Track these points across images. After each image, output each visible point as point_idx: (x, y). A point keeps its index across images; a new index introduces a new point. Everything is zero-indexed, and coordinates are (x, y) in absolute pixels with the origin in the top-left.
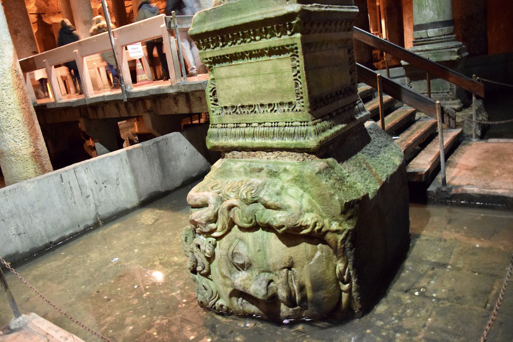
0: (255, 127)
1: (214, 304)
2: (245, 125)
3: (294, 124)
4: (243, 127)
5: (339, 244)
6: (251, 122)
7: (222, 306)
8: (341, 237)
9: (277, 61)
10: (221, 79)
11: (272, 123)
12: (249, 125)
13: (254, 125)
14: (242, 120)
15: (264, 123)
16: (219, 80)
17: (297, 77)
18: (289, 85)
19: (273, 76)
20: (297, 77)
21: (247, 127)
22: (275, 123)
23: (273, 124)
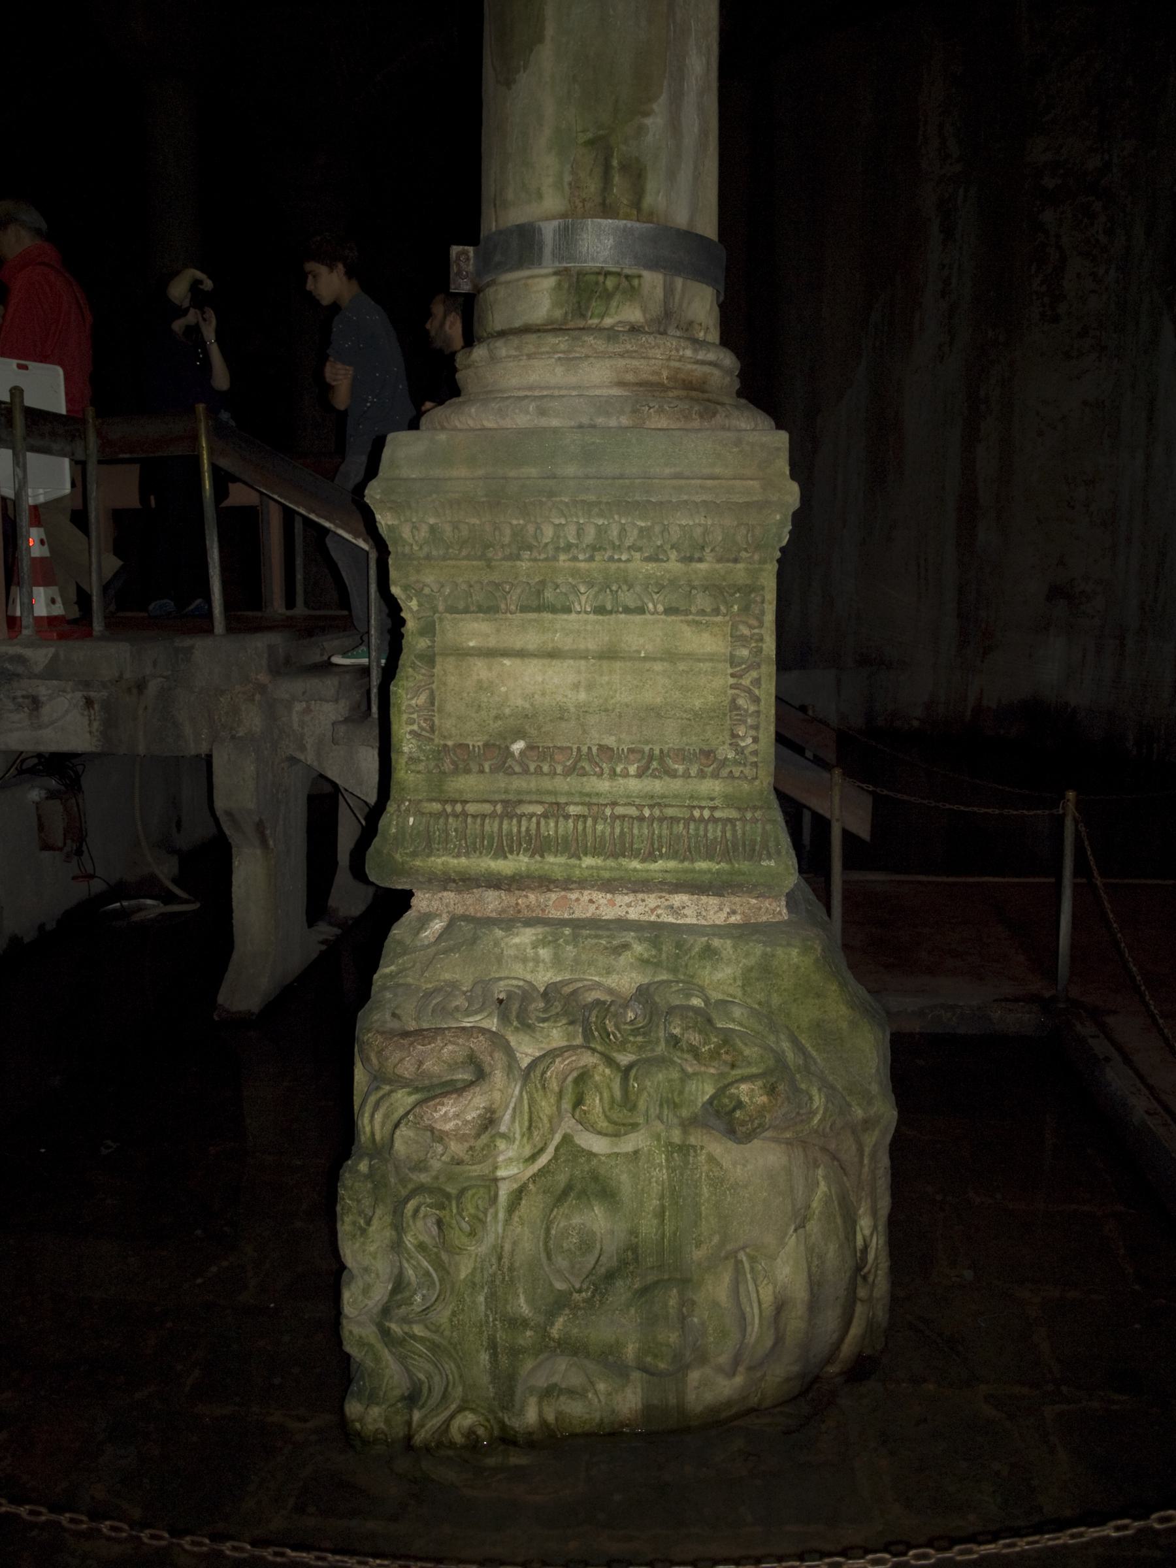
0: (578, 817)
1: (448, 1422)
2: (539, 810)
3: (718, 814)
4: (532, 815)
5: (866, 1161)
6: (562, 800)
7: (470, 1433)
8: (870, 1140)
9: (685, 627)
10: (462, 654)
11: (640, 807)
12: (556, 810)
13: (573, 810)
14: (529, 792)
15: (614, 804)
16: (451, 659)
17: (746, 682)
18: (711, 698)
19: (658, 667)
20: (746, 682)
21: (545, 816)
22: (651, 807)
23: (647, 813)
